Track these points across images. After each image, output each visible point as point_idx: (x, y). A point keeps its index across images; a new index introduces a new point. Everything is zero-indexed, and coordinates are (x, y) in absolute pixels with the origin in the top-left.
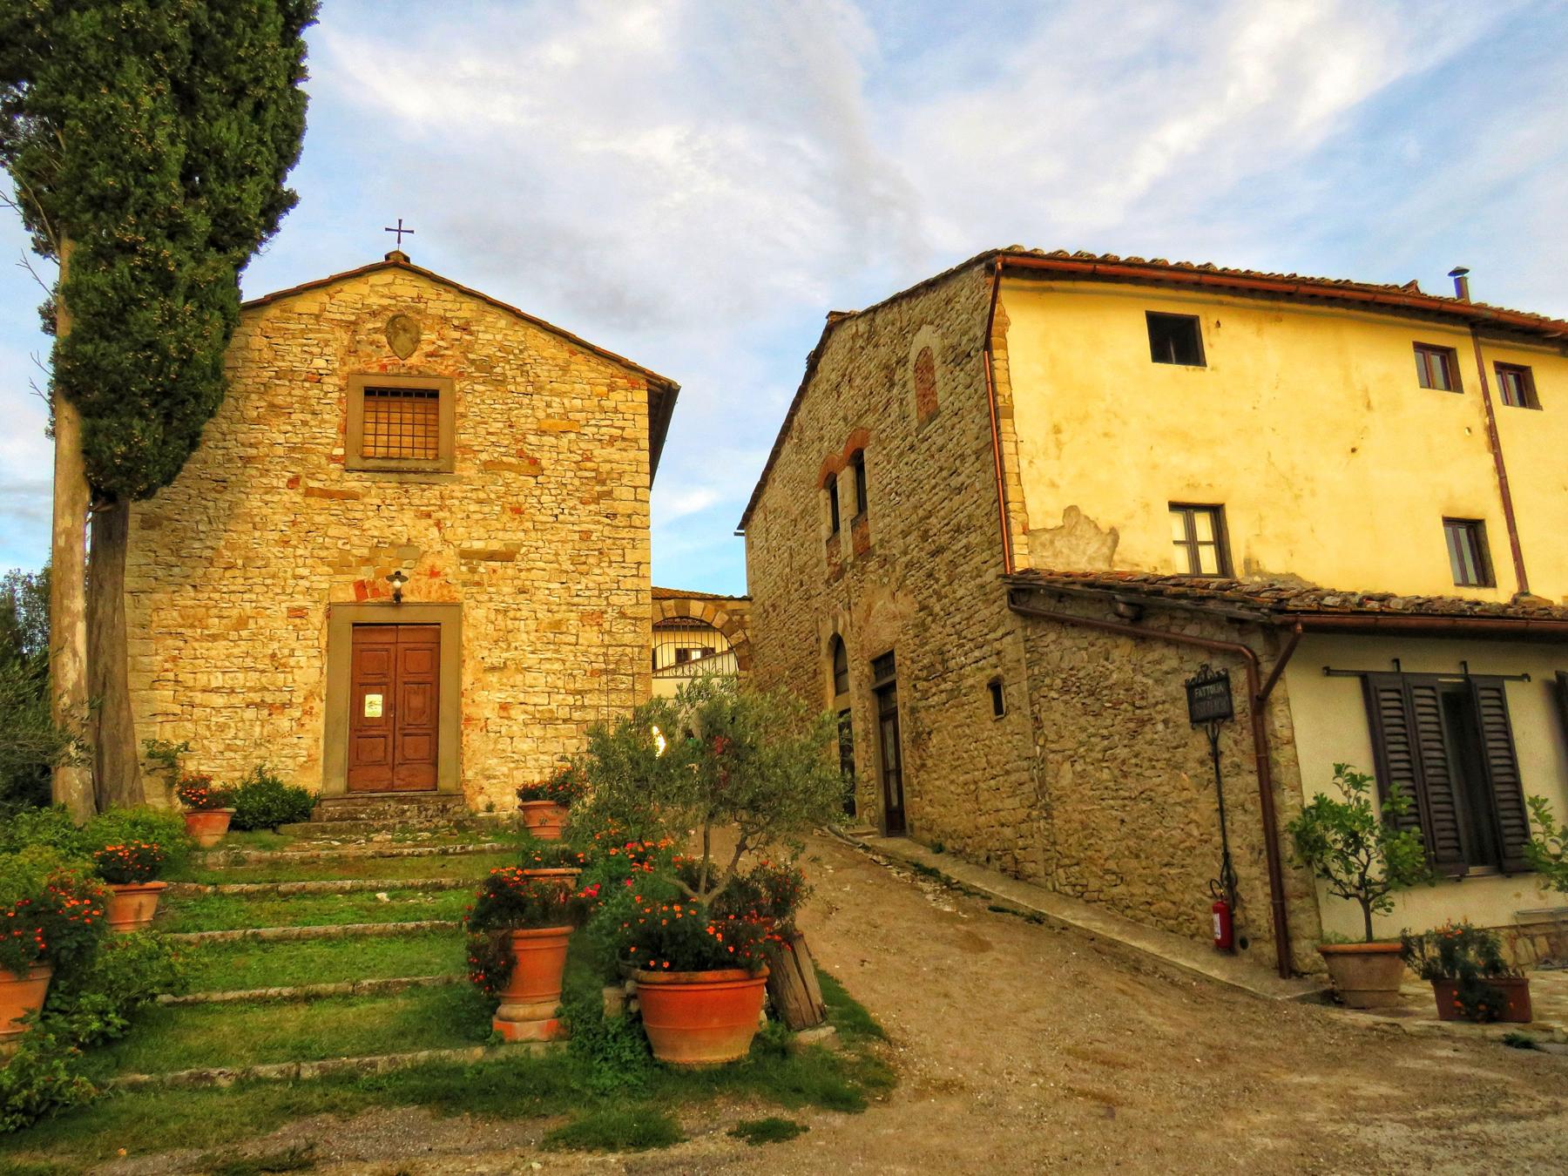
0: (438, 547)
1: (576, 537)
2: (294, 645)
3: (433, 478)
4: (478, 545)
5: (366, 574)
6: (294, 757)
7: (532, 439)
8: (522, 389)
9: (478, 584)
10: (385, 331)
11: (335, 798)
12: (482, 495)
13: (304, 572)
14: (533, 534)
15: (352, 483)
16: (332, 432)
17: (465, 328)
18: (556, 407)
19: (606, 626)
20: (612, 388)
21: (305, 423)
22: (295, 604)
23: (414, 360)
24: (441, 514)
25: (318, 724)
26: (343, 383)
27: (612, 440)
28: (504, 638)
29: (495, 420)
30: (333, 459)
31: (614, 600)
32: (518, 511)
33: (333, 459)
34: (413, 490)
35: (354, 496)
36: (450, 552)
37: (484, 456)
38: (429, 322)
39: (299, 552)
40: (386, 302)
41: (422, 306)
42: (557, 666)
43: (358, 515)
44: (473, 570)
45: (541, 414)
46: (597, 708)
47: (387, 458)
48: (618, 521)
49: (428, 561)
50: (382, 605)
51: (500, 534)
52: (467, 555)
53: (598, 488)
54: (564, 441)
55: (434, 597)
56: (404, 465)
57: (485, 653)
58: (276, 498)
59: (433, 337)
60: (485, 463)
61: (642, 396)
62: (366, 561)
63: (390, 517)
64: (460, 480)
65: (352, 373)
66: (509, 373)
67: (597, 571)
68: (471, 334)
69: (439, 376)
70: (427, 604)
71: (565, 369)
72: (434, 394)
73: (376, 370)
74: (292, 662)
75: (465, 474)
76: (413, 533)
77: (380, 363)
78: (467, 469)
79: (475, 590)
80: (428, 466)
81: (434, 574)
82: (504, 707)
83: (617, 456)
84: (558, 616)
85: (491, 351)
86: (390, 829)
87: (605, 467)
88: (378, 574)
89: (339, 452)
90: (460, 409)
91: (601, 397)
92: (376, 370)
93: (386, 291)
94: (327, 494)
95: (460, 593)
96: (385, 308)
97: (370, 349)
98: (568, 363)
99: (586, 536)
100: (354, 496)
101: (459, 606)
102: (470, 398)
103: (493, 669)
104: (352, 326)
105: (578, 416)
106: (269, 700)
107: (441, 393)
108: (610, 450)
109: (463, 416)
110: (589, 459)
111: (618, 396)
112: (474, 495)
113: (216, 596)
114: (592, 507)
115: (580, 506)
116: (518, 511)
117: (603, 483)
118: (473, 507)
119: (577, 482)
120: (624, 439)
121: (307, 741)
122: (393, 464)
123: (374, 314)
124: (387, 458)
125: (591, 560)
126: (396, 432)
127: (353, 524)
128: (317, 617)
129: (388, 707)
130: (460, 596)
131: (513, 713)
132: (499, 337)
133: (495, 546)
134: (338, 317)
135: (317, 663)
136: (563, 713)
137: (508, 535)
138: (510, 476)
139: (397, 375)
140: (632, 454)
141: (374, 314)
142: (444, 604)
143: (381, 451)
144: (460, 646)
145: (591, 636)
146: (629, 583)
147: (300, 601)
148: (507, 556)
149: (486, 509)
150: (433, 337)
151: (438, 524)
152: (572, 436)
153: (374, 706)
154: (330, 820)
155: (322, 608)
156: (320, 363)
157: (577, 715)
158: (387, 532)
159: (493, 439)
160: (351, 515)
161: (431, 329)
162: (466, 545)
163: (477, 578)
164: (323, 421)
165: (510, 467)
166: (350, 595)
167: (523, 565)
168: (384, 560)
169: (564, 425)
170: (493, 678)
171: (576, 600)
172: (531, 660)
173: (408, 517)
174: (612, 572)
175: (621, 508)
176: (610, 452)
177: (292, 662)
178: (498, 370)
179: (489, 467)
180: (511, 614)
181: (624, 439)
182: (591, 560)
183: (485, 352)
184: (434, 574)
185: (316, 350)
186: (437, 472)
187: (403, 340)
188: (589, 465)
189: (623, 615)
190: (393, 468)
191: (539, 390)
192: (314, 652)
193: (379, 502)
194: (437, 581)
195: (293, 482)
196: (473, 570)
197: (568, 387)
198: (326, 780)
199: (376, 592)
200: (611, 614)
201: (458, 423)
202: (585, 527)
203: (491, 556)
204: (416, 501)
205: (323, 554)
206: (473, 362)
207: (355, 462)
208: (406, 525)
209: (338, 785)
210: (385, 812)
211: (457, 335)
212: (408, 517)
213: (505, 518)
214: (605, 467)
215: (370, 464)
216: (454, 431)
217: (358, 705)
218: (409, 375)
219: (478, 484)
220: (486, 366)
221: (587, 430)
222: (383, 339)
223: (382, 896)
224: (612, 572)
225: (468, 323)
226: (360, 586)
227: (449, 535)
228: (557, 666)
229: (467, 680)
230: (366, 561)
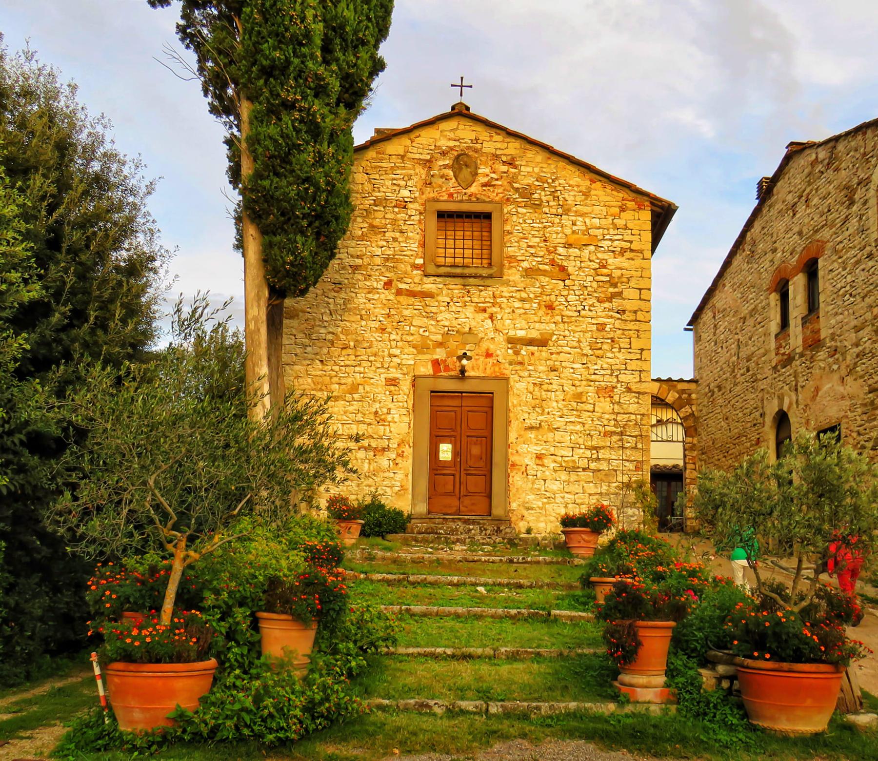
0: (491, 335)
1: (594, 328)
2: (391, 405)
3: (488, 282)
4: (521, 334)
5: (440, 354)
6: (391, 487)
7: (561, 250)
8: (554, 211)
9: (521, 363)
10: (452, 167)
11: (420, 517)
12: (524, 295)
13: (397, 352)
14: (561, 326)
15: (429, 285)
16: (414, 246)
17: (511, 163)
18: (580, 226)
19: (616, 398)
20: (623, 209)
21: (395, 239)
22: (391, 376)
23: (473, 189)
24: (494, 309)
25: (407, 464)
26: (421, 208)
27: (623, 251)
28: (539, 405)
29: (534, 236)
30: (415, 267)
31: (622, 378)
32: (550, 307)
33: (415, 267)
34: (473, 290)
35: (431, 295)
36: (500, 338)
37: (525, 265)
38: (483, 159)
39: (393, 337)
40: (452, 144)
41: (478, 146)
42: (579, 427)
43: (434, 310)
44: (517, 353)
45: (568, 231)
46: (609, 461)
47: (454, 266)
48: (628, 316)
49: (485, 345)
51: (537, 325)
52: (512, 341)
53: (611, 290)
54: (586, 253)
55: (489, 372)
56: (467, 271)
57: (526, 416)
58: (376, 296)
60: (526, 270)
61: (646, 216)
62: (440, 345)
63: (456, 311)
64: (507, 283)
65: (428, 200)
66: (544, 199)
67: (610, 355)
68: (515, 167)
69: (491, 202)
70: (483, 378)
71: (586, 194)
72: (488, 216)
73: (446, 198)
74: (389, 418)
75: (511, 278)
76: (473, 324)
77: (449, 192)
78: (513, 275)
79: (518, 367)
80: (485, 272)
81: (489, 355)
82: (539, 457)
83: (626, 264)
84: (579, 390)
85: (530, 180)
86: (463, 542)
87: (617, 273)
88: (450, 355)
89: (420, 261)
90: (507, 228)
91: (614, 216)
92: (446, 198)
93: (452, 135)
94: (412, 294)
95: (508, 370)
96: (452, 149)
98: (589, 189)
99: (601, 327)
100: (431, 295)
101: (507, 379)
102: (515, 218)
103: (531, 428)
104: (428, 164)
105: (599, 232)
106: (374, 445)
107: (494, 216)
108: (620, 259)
109: (510, 233)
110: (604, 267)
112: (518, 295)
113: (336, 368)
114: (607, 305)
115: (597, 304)
116: (550, 307)
117: (615, 285)
118: (517, 304)
119: (595, 285)
120: (632, 251)
121: (400, 476)
122: (458, 271)
123: (444, 154)
124: (454, 266)
125: (605, 347)
126: (461, 246)
127: (431, 316)
128: (406, 386)
129: (456, 453)
131: (546, 461)
132: (536, 170)
133: (534, 334)
134: (417, 156)
135: (406, 419)
136: (583, 463)
137: (543, 326)
138: (545, 280)
139: (461, 201)
141: (444, 154)
142: (496, 378)
143: (449, 261)
144: (508, 410)
145: (604, 405)
146: (633, 365)
147: (394, 373)
148: (542, 343)
149: (527, 306)
151: (491, 317)
152: (592, 248)
153: (446, 452)
154: (420, 533)
155: (409, 378)
156: (405, 193)
157: (593, 466)
158: (455, 323)
159: (532, 251)
160: (429, 309)
161: (486, 164)
162: (512, 333)
163: (520, 359)
164: (408, 238)
165: (544, 273)
166: (428, 370)
167: (554, 350)
168: (452, 344)
169: (585, 239)
170: (532, 435)
171: (593, 377)
172: (559, 422)
173: (469, 311)
175: (629, 305)
177: (389, 418)
178: (536, 196)
179: (529, 273)
180: (545, 387)
181: (632, 251)
182: (605, 347)
183: (526, 182)
184: (489, 355)
185: (403, 183)
186: (491, 277)
187: (466, 173)
188: (605, 271)
189: (629, 390)
190: (458, 274)
191: (567, 212)
192: (404, 411)
193: (448, 300)
195: (388, 284)
196: (517, 353)
197: (589, 209)
198: (413, 505)
199: (447, 369)
200: (620, 389)
201: (506, 238)
202: (601, 320)
203: (531, 342)
204: (476, 300)
205: (410, 338)
206: (517, 190)
207: (431, 269)
208: (469, 318)
209: (422, 508)
210: (457, 530)
211: (505, 168)
212: (469, 311)
213: (541, 313)
214: (617, 273)
215: (442, 270)
216: (503, 245)
217: (434, 452)
218: (469, 201)
219: (521, 286)
220: (526, 193)
222: (451, 173)
223: (481, 589)
225: (513, 159)
226: (436, 363)
227: (499, 325)
228: (579, 427)
229: (512, 436)
230: (440, 345)
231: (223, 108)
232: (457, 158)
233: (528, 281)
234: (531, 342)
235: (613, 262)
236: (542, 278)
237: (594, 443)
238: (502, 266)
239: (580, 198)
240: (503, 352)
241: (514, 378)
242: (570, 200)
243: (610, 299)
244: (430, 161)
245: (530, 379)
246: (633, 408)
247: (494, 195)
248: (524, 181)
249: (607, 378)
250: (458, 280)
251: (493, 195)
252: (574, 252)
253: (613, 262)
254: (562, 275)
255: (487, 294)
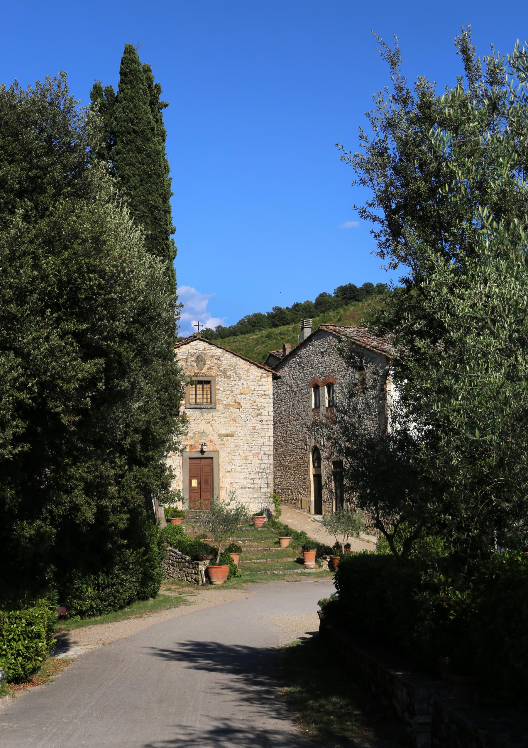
0: (212, 433)
3: (211, 410)
4: (223, 432)
7: (238, 396)
12: (224, 416)
14: (239, 428)
17: (218, 359)
18: (245, 385)
19: (260, 458)
20: (262, 377)
27: (262, 395)
28: (231, 462)
31: (262, 449)
32: (235, 421)
34: (204, 414)
36: (216, 435)
37: (225, 403)
40: (195, 351)
42: (246, 471)
44: (222, 440)
45: (241, 388)
46: (258, 484)
48: (264, 423)
49: (210, 437)
50: (197, 452)
51: (230, 428)
52: (220, 435)
54: (247, 397)
55: (211, 449)
56: (202, 406)
59: (209, 362)
60: (225, 405)
64: (218, 411)
71: (248, 372)
72: (209, 382)
78: (220, 407)
80: (209, 407)
82: (231, 484)
83: (263, 401)
84: (246, 455)
85: (226, 366)
87: (260, 405)
88: (196, 442)
90: (217, 387)
93: (195, 347)
95: (218, 448)
96: (195, 353)
97: (191, 368)
101: (218, 451)
103: (228, 472)
107: (212, 382)
108: (261, 399)
111: (264, 380)
112: (222, 416)
114: (256, 418)
116: (235, 421)
117: (259, 410)
118: (222, 420)
122: (199, 406)
123: (192, 356)
124: (197, 404)
125: (256, 436)
129: (199, 483)
130: (218, 449)
133: (229, 432)
136: (248, 485)
140: (268, 400)
141: (192, 356)
142: (214, 451)
143: (194, 401)
144: (219, 465)
145: (256, 461)
146: (267, 443)
148: (232, 436)
149: (225, 420)
150: (209, 362)
151: (211, 425)
153: (194, 483)
157: (252, 486)
158: (197, 428)
162: (220, 432)
167: (237, 438)
168: (197, 437)
169: (247, 391)
172: (239, 469)
174: (262, 440)
175: (265, 418)
176: (261, 400)
179: (226, 406)
184: (211, 442)
186: (211, 408)
187: (201, 364)
188: (255, 404)
189: (265, 454)
191: (240, 379)
194: (212, 444)
196: (222, 440)
199: (195, 448)
200: (262, 453)
202: (254, 425)
203: (227, 436)
206: (221, 371)
211: (216, 361)
212: (203, 423)
214: (260, 405)
215: (192, 406)
216: (216, 394)
218: (202, 376)
219: (223, 412)
220: (224, 372)
221: (254, 392)
224: (262, 440)
227: (215, 429)
228: (246, 471)
231: (230, 327)
232: (198, 357)
233: (226, 410)
234: (227, 436)
235: (258, 400)
236: (231, 408)
237: (252, 477)
238: (216, 404)
239: (245, 373)
240: (217, 440)
241: (221, 451)
242: (242, 374)
243: (257, 416)
244: (186, 359)
245: (228, 451)
246: (267, 461)
247: (212, 373)
248: (224, 367)
249: (256, 449)
250: (199, 410)
251: (211, 373)
252: (243, 396)
253: (258, 400)
254: (239, 407)
255: (210, 415)
